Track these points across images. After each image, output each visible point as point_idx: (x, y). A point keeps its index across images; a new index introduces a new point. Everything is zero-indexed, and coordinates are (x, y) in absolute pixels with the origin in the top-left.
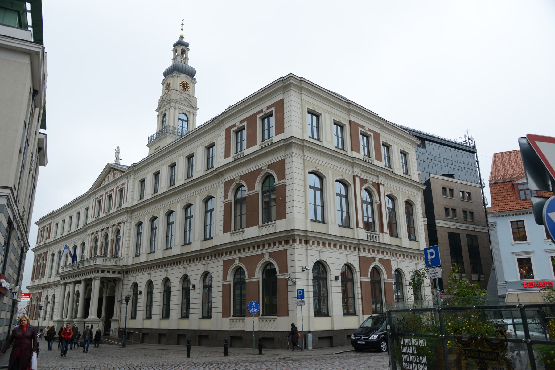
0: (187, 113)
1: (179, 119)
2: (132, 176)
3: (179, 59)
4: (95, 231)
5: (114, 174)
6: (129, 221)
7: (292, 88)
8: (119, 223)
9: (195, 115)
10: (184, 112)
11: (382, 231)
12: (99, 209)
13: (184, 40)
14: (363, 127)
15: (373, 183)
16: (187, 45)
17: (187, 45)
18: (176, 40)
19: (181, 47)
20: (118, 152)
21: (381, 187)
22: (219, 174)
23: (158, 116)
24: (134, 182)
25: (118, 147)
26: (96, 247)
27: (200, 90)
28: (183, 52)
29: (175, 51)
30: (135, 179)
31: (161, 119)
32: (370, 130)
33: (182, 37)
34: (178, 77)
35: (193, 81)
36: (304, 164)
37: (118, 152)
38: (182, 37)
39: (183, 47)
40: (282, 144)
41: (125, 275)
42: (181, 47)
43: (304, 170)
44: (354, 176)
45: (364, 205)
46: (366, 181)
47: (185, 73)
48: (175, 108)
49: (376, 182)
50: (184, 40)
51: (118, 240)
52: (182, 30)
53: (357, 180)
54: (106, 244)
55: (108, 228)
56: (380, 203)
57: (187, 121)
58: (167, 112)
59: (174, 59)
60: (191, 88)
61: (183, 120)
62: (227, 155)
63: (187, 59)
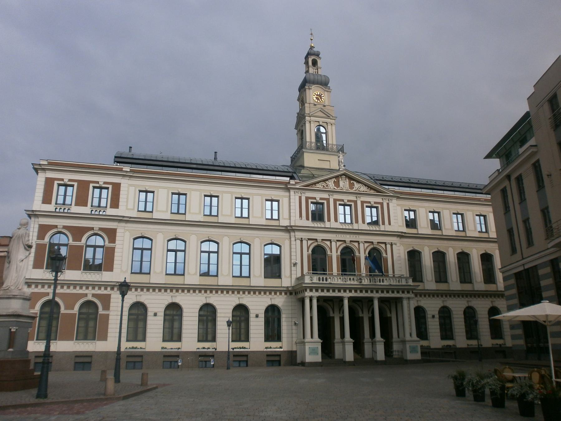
0: (325, 125)
3: (311, 70)
10: (321, 123)
13: (314, 49)
16: (318, 55)
17: (318, 55)
19: (312, 58)
23: (297, 134)
29: (307, 63)
31: (300, 137)
33: (312, 48)
34: (309, 89)
39: (313, 57)
42: (312, 58)
47: (317, 84)
48: (310, 122)
50: (314, 49)
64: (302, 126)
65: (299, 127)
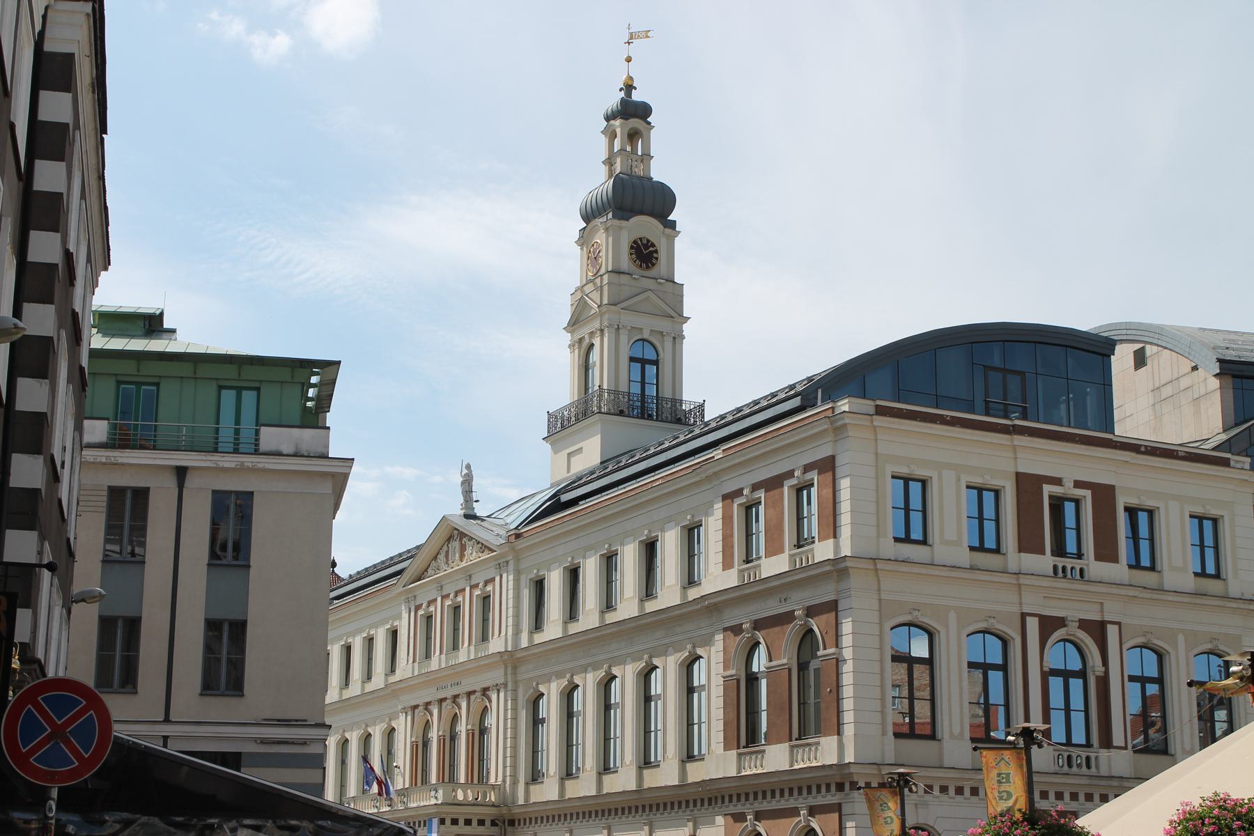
1: (632, 359)
2: (511, 566)
4: (421, 701)
5: (463, 548)
6: (510, 686)
7: (850, 434)
8: (485, 691)
9: (678, 338)
10: (646, 336)
11: (1107, 742)
12: (428, 638)
13: (636, 96)
14: (1058, 481)
15: (1084, 625)
18: (614, 99)
20: (467, 483)
21: (1112, 631)
22: (714, 606)
24: (517, 581)
25: (468, 467)
26: (426, 743)
27: (691, 258)
28: (633, 136)
29: (612, 136)
30: (518, 573)
32: (1078, 484)
33: (629, 88)
35: (668, 231)
36: (880, 611)
37: (467, 483)
38: (629, 88)
40: (828, 568)
41: (509, 829)
43: (881, 624)
44: (1023, 616)
45: (1056, 683)
46: (1061, 622)
47: (641, 213)
49: (1097, 618)
51: (483, 731)
52: (629, 60)
53: (1033, 625)
54: (453, 737)
55: (456, 697)
56: (1107, 672)
57: (656, 363)
58: (597, 341)
59: (609, 162)
60: (662, 255)
61: (644, 362)
62: (727, 564)
63: (647, 156)
64: (592, 334)
65: (584, 332)
